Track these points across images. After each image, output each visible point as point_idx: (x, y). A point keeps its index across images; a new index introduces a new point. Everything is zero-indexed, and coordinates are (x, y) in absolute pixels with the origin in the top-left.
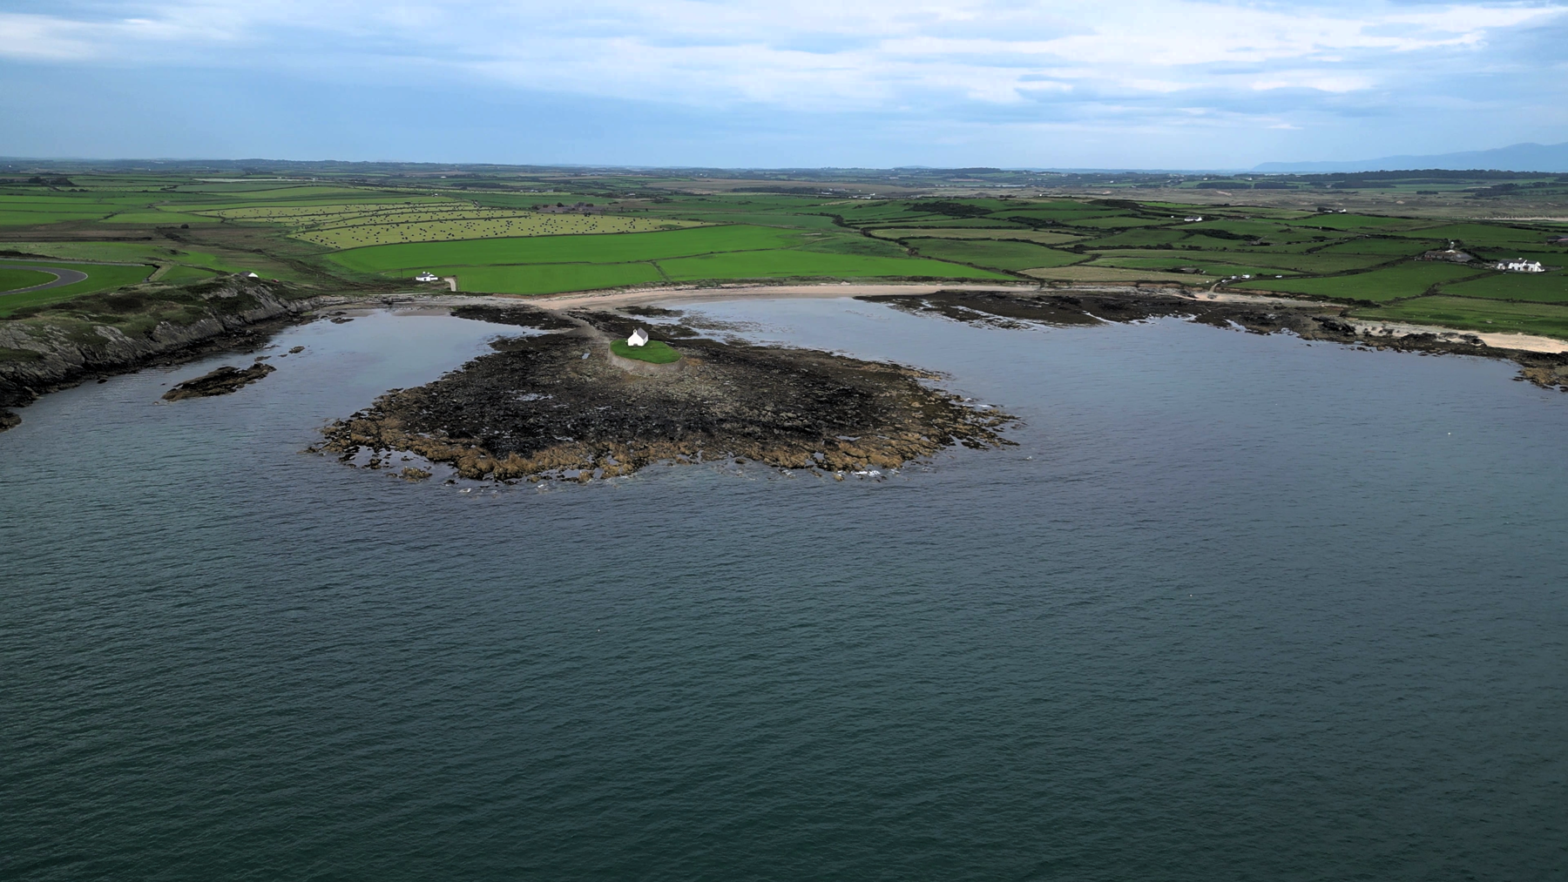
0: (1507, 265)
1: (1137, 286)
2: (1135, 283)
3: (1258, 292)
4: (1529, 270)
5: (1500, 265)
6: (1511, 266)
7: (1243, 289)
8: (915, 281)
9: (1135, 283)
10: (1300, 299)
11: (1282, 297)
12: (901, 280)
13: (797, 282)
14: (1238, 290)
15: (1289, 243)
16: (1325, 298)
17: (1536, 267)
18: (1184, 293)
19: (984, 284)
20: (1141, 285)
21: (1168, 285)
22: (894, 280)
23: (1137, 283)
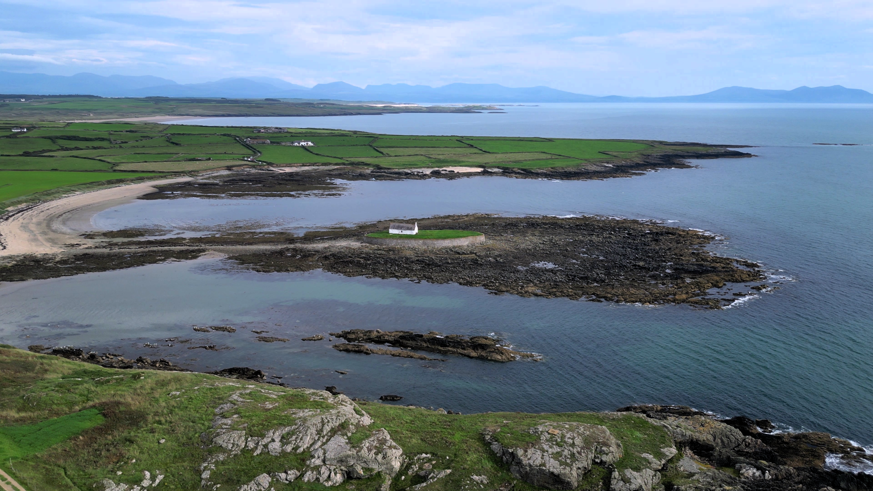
0: (299, 143)
1: (230, 170)
2: (226, 168)
3: (296, 165)
4: (309, 145)
5: (296, 143)
6: (301, 143)
7: (287, 164)
8: (112, 183)
9: (226, 168)
10: (318, 166)
11: (309, 166)
12: (104, 184)
13: (49, 198)
14: (285, 165)
15: (137, 141)
16: (330, 164)
17: (310, 144)
18: (260, 170)
19: (157, 180)
20: (234, 168)
21: (244, 166)
22: (99, 185)
23: (229, 168)
